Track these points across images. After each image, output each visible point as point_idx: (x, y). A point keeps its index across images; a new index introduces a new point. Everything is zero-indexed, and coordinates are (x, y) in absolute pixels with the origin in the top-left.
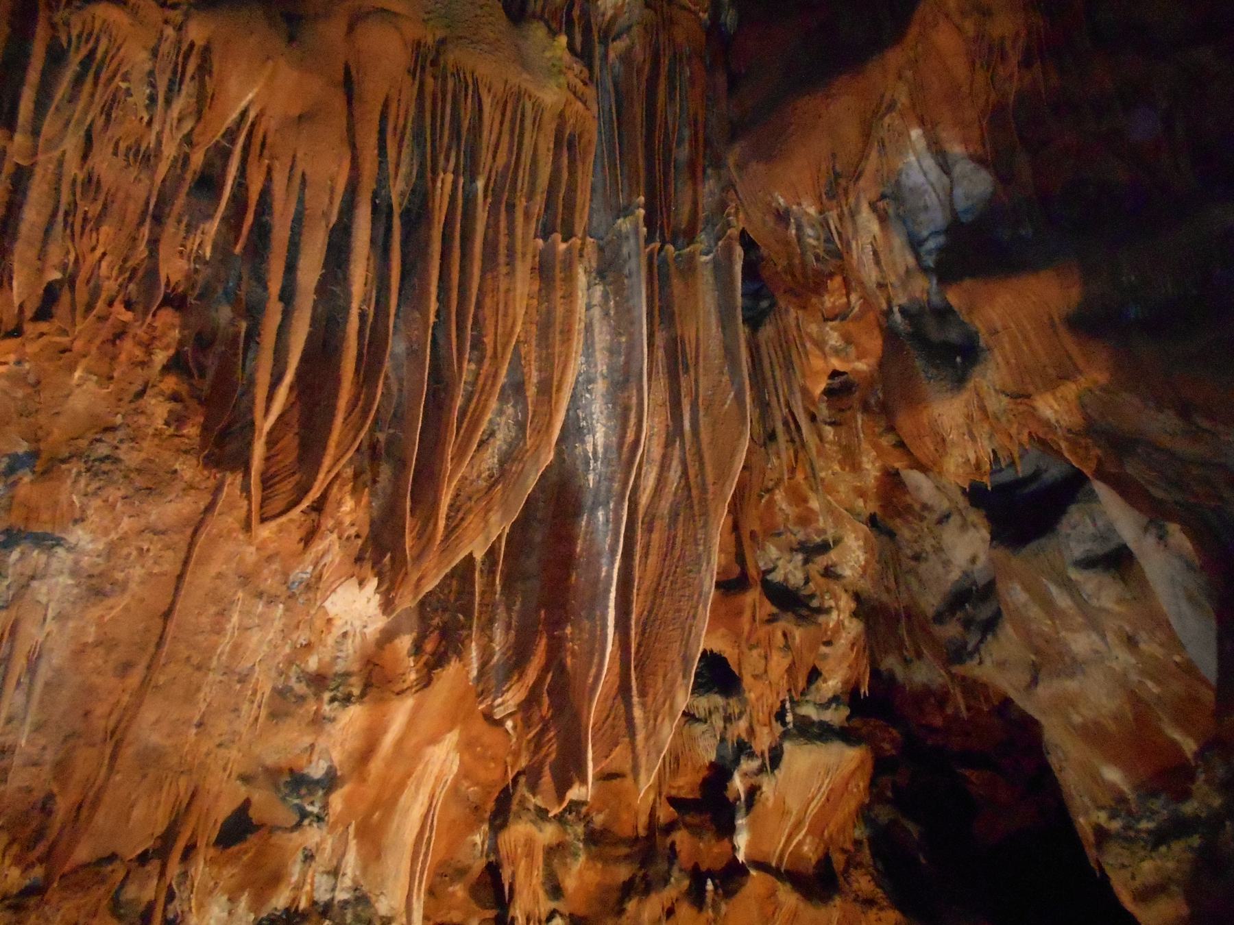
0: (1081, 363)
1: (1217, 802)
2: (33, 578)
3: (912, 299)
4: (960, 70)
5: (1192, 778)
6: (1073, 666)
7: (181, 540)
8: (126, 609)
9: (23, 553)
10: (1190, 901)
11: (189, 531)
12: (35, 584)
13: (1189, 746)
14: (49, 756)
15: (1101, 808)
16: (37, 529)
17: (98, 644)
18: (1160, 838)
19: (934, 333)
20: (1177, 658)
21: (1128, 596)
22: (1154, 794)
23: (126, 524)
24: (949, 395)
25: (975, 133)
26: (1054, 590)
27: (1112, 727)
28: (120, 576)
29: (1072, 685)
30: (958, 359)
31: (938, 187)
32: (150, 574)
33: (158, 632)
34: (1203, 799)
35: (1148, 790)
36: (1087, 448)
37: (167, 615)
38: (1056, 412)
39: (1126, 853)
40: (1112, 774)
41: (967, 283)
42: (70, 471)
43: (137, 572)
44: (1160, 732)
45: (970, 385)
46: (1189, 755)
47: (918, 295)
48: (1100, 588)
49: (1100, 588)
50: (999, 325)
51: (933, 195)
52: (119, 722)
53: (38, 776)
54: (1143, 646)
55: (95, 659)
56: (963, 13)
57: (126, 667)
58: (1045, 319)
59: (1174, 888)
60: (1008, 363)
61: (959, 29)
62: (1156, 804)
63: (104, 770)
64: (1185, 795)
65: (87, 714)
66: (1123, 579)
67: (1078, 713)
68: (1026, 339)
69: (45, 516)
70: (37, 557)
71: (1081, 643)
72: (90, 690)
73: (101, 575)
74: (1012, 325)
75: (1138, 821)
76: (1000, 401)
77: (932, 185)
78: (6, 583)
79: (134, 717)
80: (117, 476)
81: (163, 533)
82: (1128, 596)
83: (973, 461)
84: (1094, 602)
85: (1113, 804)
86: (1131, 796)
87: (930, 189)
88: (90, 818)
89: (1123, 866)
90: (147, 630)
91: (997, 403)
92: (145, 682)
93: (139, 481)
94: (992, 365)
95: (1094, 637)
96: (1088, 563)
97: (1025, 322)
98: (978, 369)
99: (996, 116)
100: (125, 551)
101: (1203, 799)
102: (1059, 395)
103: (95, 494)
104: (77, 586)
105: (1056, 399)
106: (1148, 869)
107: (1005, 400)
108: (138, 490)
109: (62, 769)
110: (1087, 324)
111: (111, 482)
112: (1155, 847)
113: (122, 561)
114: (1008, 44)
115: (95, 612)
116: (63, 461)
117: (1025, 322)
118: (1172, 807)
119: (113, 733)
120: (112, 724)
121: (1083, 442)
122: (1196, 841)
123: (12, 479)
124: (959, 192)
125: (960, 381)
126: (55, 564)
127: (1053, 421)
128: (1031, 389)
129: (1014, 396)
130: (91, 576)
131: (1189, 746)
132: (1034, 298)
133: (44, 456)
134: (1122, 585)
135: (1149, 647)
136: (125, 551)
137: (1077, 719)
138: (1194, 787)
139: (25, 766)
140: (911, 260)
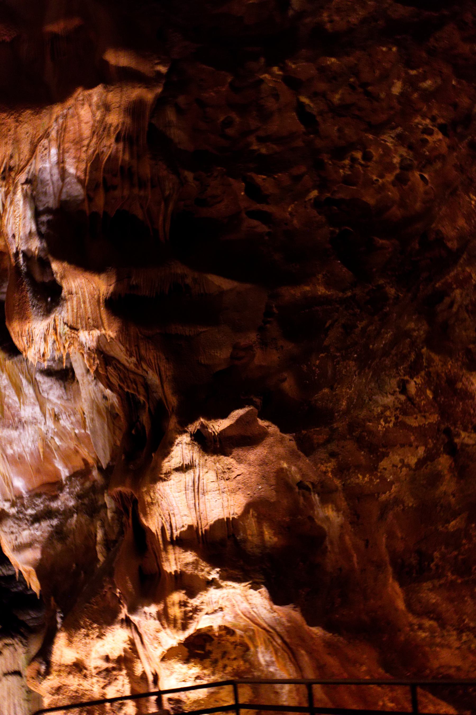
0: (106, 324)
1: (72, 503)
3: (29, 250)
4: (87, 132)
5: (61, 488)
6: (19, 424)
10: (43, 552)
13: (64, 473)
15: (7, 500)
18: (36, 519)
19: (38, 277)
20: (77, 431)
21: (65, 397)
22: (39, 495)
24: (41, 318)
25: (83, 166)
26: (24, 382)
27: (28, 458)
29: (14, 434)
30: (49, 299)
31: (56, 185)
34: (66, 500)
35: (35, 494)
36: (94, 359)
38: (86, 339)
39: (16, 526)
40: (19, 484)
41: (65, 264)
44: (52, 464)
45: (52, 316)
46: (63, 478)
47: (33, 249)
48: (51, 388)
49: (51, 388)
50: (74, 291)
51: (51, 188)
54: (62, 422)
56: (98, 108)
58: (96, 296)
59: (37, 545)
60: (73, 311)
61: (94, 115)
62: (38, 501)
64: (55, 498)
66: (65, 388)
67: (12, 448)
68: (84, 302)
71: (29, 411)
74: (80, 293)
75: (26, 510)
76: (64, 329)
77: (53, 183)
82: (65, 397)
83: (42, 352)
84: (45, 395)
85: (14, 498)
86: (25, 495)
87: (51, 184)
89: (12, 533)
91: (62, 329)
94: (65, 309)
95: (37, 409)
96: (48, 373)
97: (87, 295)
98: (58, 309)
99: (96, 161)
101: (66, 500)
102: (91, 333)
105: (89, 334)
106: (25, 535)
107: (67, 329)
110: (113, 305)
112: (33, 523)
114: (112, 129)
117: (87, 295)
118: (47, 503)
121: (93, 355)
122: (55, 522)
124: (64, 190)
125: (48, 312)
127: (84, 343)
128: (79, 326)
129: (72, 328)
131: (64, 473)
132: (94, 285)
134: (64, 391)
135: (65, 422)
137: (10, 451)
138: (61, 495)
140: (34, 228)
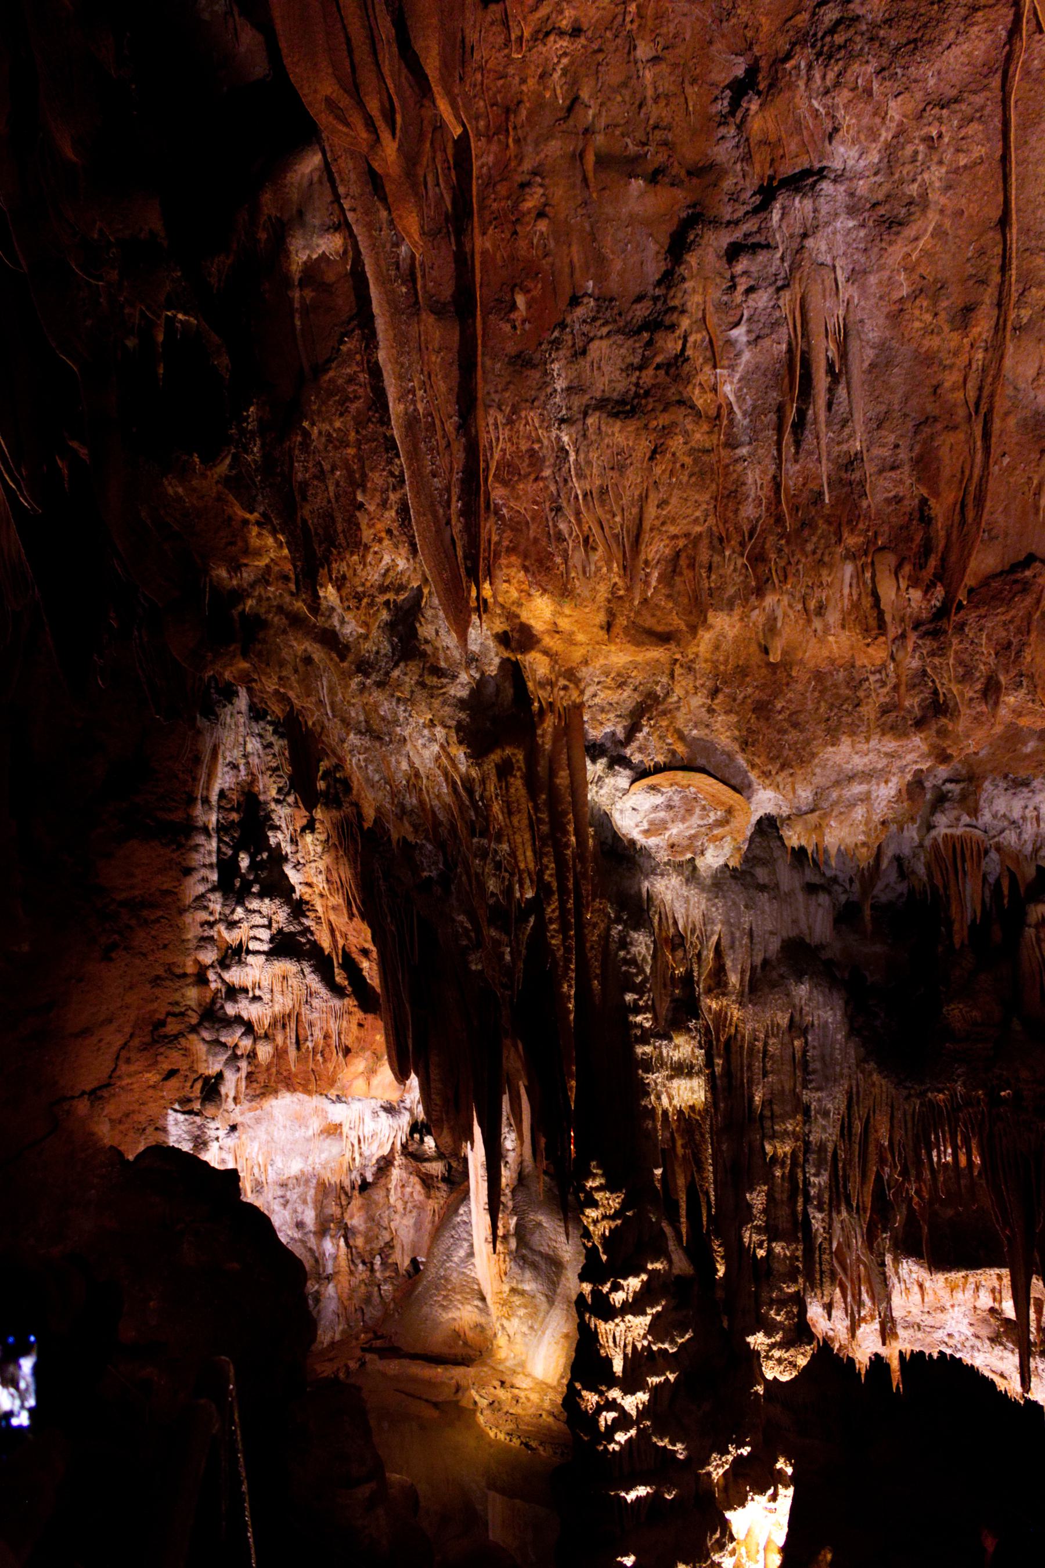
2: (805, 236)
7: (986, 99)
8: (939, 233)
9: (783, 208)
11: (996, 82)
12: (810, 243)
14: (903, 455)
16: (787, 169)
17: (915, 296)
23: (895, 109)
28: (913, 189)
32: (957, 171)
33: (998, 250)
37: (1004, 222)
42: (797, 67)
43: (935, 175)
52: (980, 389)
53: (901, 482)
55: (920, 317)
57: (966, 313)
63: (979, 457)
65: (936, 388)
69: (793, 146)
70: (801, 206)
72: (928, 359)
73: (888, 196)
78: (779, 255)
79: (997, 376)
80: (859, 43)
81: (956, 100)
88: (979, 516)
90: (981, 253)
92: (999, 328)
93: (894, 37)
100: (909, 150)
103: (837, 84)
104: (863, 226)
108: (895, 52)
109: (925, 465)
111: (851, 57)
113: (908, 167)
115: (897, 252)
116: (788, 56)
119: (977, 404)
120: (972, 395)
123: (739, 115)
126: (824, 209)
130: (874, 205)
133: (763, 64)
136: (909, 150)
139: (881, 472)
